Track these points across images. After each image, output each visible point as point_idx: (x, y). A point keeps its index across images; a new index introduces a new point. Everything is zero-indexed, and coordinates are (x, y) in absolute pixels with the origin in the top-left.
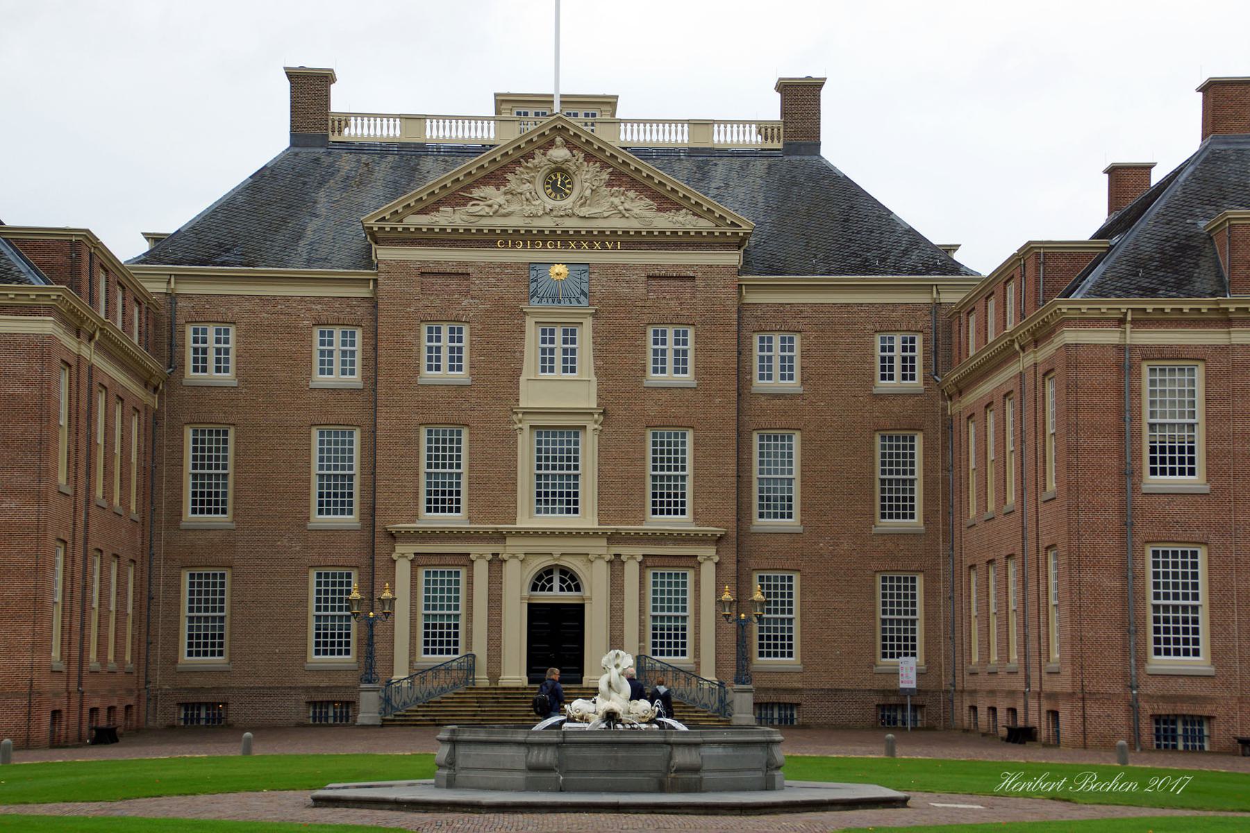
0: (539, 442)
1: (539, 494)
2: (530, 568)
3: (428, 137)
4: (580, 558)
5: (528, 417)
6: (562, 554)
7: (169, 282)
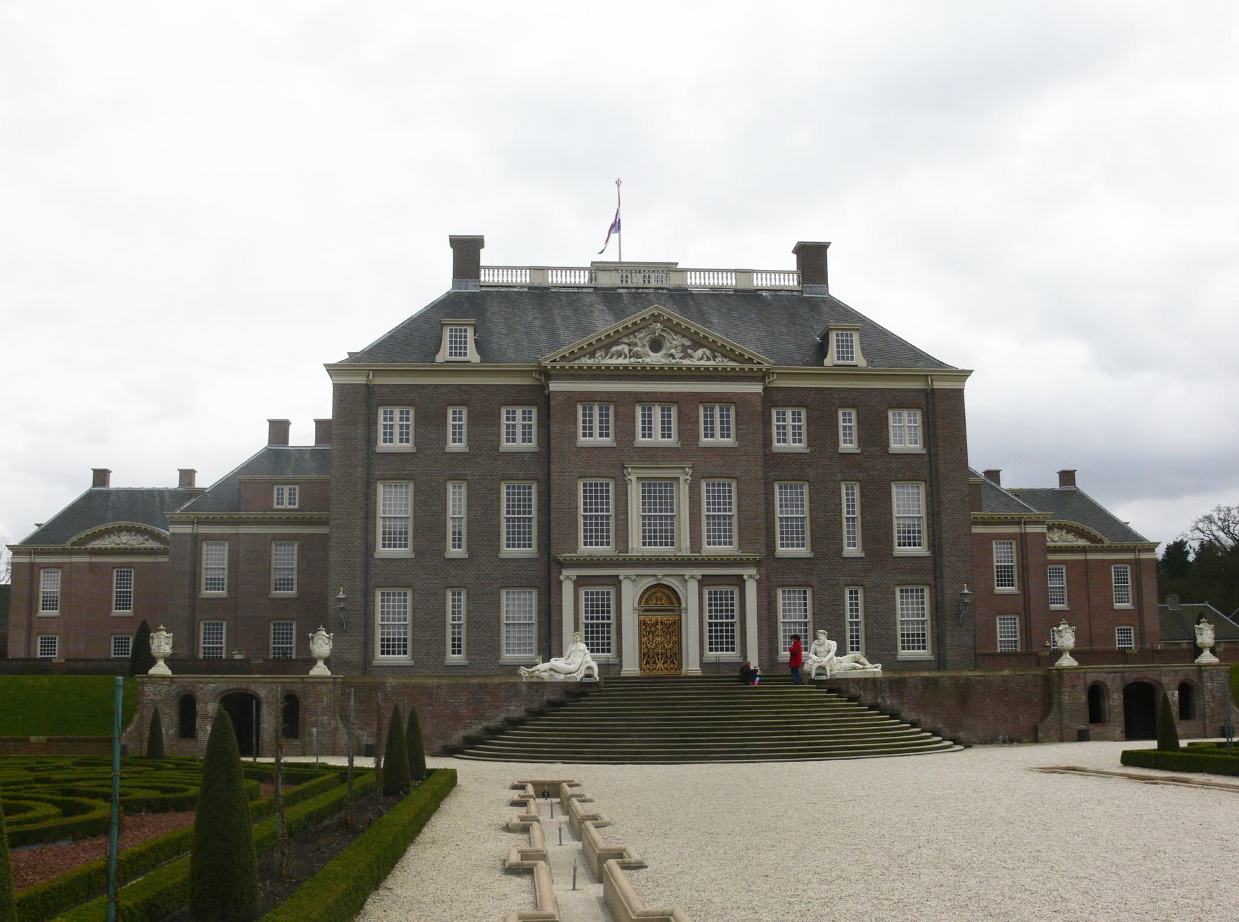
0: (644, 491)
1: (644, 531)
2: (639, 587)
3: (550, 282)
4: (678, 578)
5: (635, 471)
6: (664, 576)
7: (368, 376)
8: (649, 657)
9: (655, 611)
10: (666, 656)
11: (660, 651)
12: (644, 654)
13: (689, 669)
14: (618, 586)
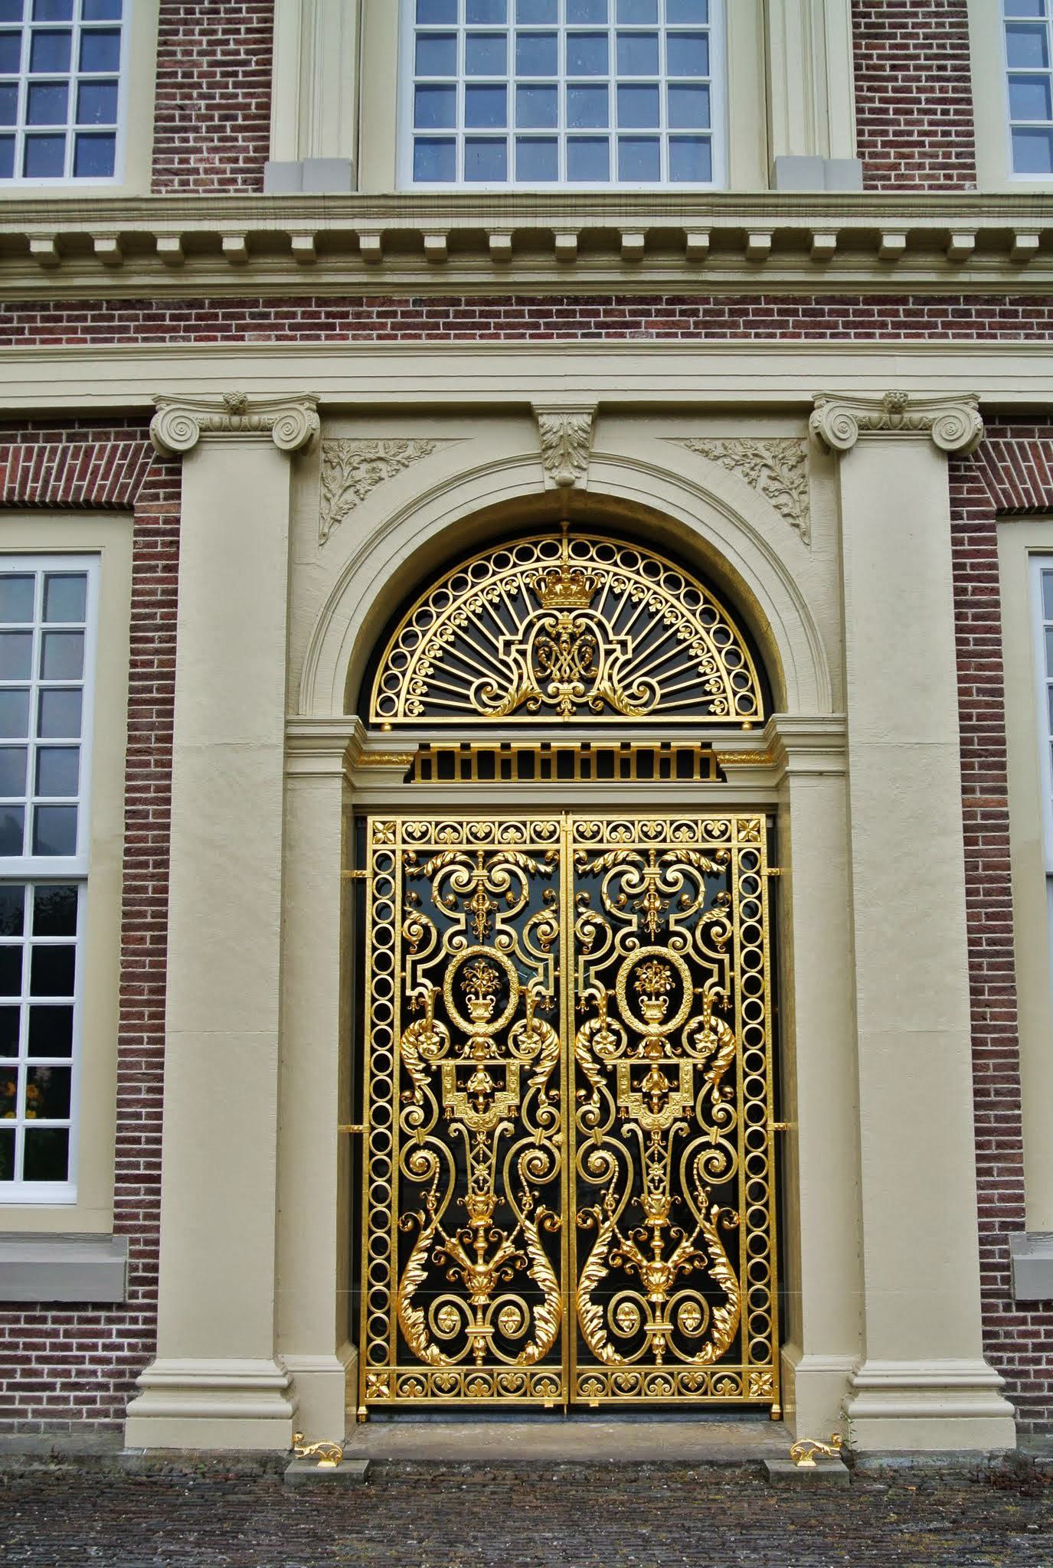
6: (607, 412)
8: (456, 1220)
9: (526, 764)
10: (632, 1219)
11: (568, 1164)
12: (411, 1196)
13: (875, 1370)
14: (154, 511)
